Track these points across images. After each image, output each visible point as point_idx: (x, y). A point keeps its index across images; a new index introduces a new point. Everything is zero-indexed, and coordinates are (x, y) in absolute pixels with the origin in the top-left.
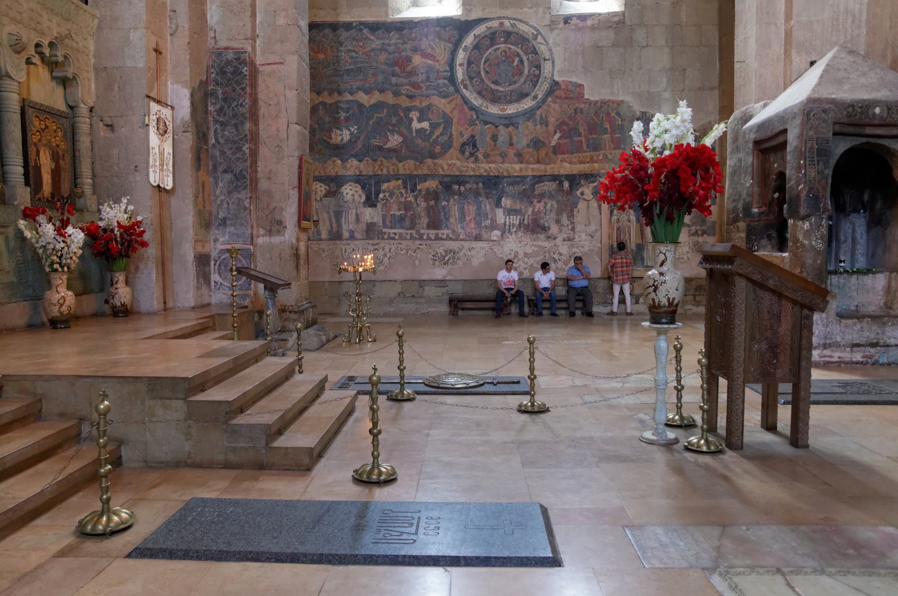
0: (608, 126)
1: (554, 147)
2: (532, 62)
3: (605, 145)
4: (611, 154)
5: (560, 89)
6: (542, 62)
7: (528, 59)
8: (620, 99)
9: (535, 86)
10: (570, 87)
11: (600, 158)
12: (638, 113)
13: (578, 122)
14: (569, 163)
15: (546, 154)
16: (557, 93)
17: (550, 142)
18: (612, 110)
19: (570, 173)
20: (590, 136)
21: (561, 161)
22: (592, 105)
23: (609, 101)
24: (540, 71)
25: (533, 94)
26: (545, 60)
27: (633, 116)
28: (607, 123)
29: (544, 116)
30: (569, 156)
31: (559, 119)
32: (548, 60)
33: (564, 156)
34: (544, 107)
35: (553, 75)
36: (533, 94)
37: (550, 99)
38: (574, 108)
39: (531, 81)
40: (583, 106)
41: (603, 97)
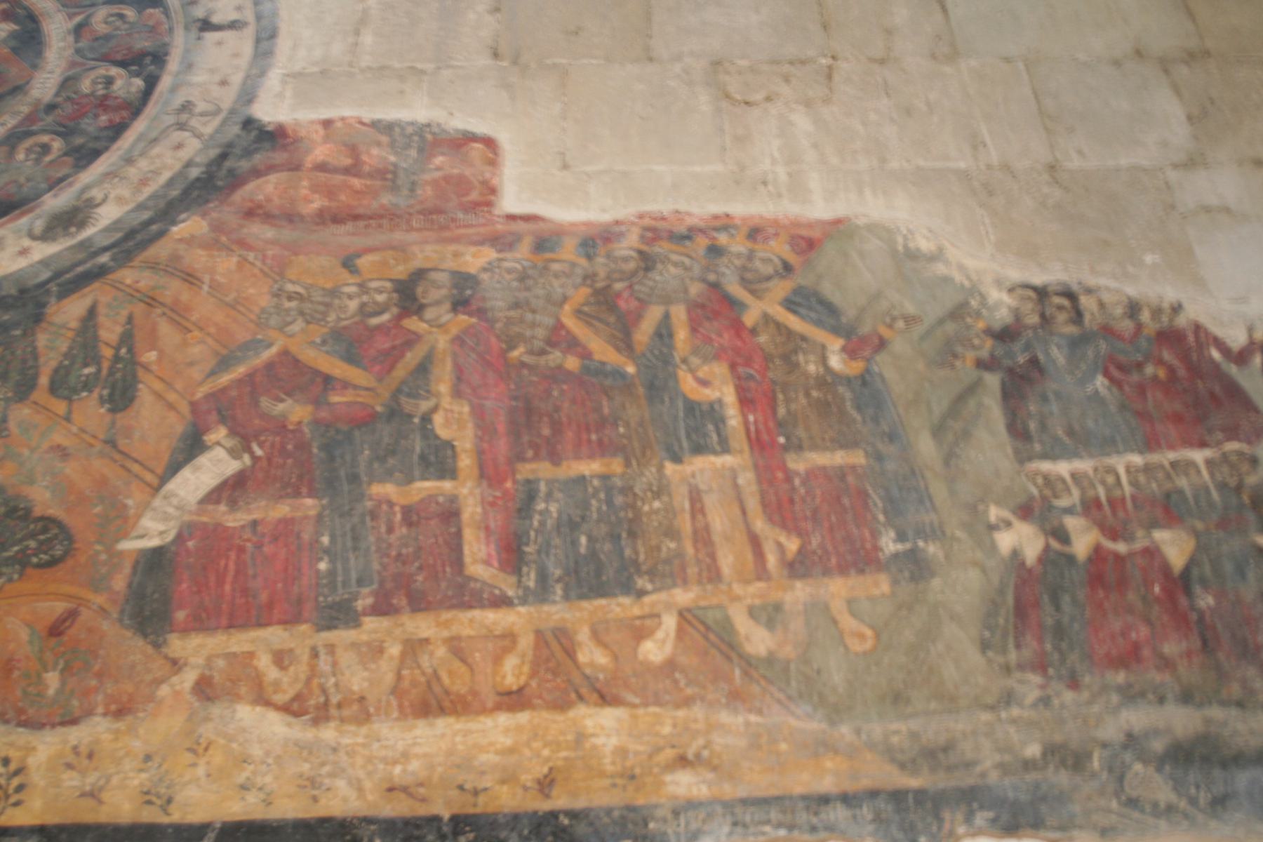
0: (729, 396)
1: (155, 561)
2: (107, 38)
3: (703, 537)
4: (770, 615)
5: (295, 167)
6: (179, 41)
7: (78, 30)
8: (819, 210)
9: (85, 156)
10: (376, 155)
11: (654, 650)
12: (996, 295)
13: (423, 369)
14: (293, 709)
15: (56, 630)
16: (267, 188)
17: (120, 521)
18: (744, 282)
19: (288, 808)
20: (542, 470)
21: (205, 689)
22: (569, 251)
23: (724, 223)
24: (151, 83)
25: (54, 202)
26: (206, 25)
27: (958, 313)
28: (719, 370)
29: (110, 332)
30: (299, 639)
31: (253, 346)
32: (233, 25)
33: (239, 642)
34: (127, 276)
35: (248, 95)
36: (54, 202)
37: (190, 225)
38: (400, 271)
39: (65, 132)
40: (475, 259)
41: (662, 205)
